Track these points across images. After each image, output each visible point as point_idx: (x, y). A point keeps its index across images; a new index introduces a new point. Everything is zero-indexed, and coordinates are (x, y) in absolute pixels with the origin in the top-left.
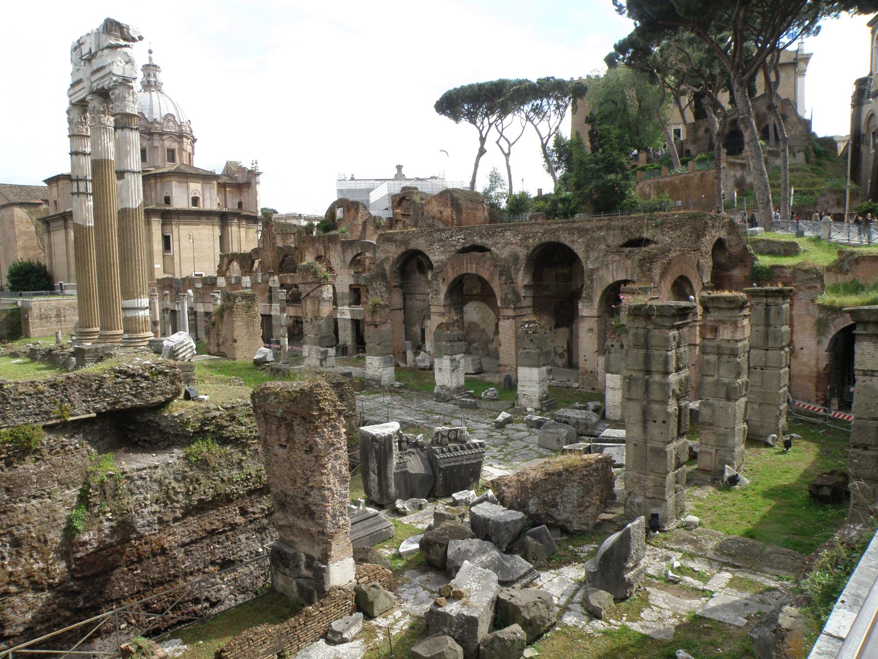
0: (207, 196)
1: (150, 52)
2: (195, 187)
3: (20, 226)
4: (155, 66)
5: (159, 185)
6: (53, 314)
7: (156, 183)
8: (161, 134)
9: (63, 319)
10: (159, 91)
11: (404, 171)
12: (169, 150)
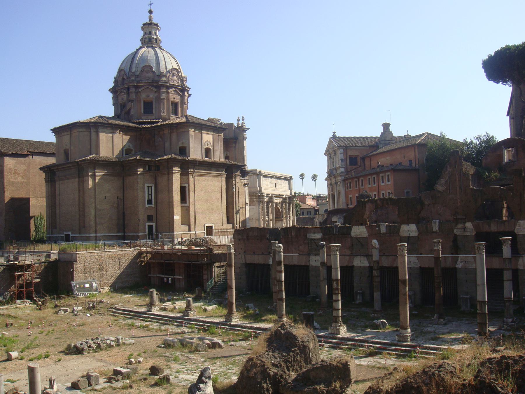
0: (217, 148)
1: (150, 12)
2: (208, 137)
3: (9, 177)
4: (156, 25)
5: (174, 136)
6: (96, 267)
7: (171, 134)
8: (168, 87)
9: (104, 273)
10: (160, 48)
11: (391, 129)
12: (173, 103)
